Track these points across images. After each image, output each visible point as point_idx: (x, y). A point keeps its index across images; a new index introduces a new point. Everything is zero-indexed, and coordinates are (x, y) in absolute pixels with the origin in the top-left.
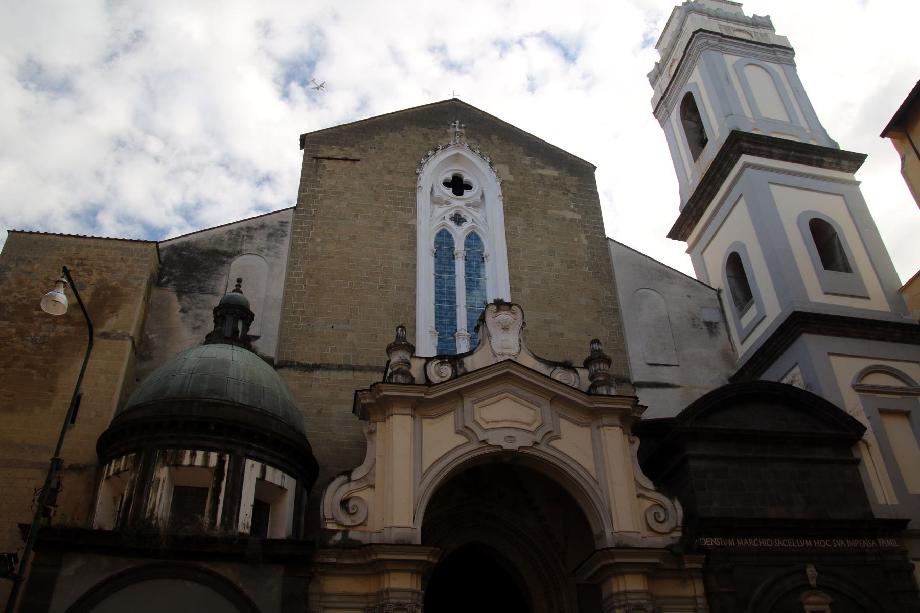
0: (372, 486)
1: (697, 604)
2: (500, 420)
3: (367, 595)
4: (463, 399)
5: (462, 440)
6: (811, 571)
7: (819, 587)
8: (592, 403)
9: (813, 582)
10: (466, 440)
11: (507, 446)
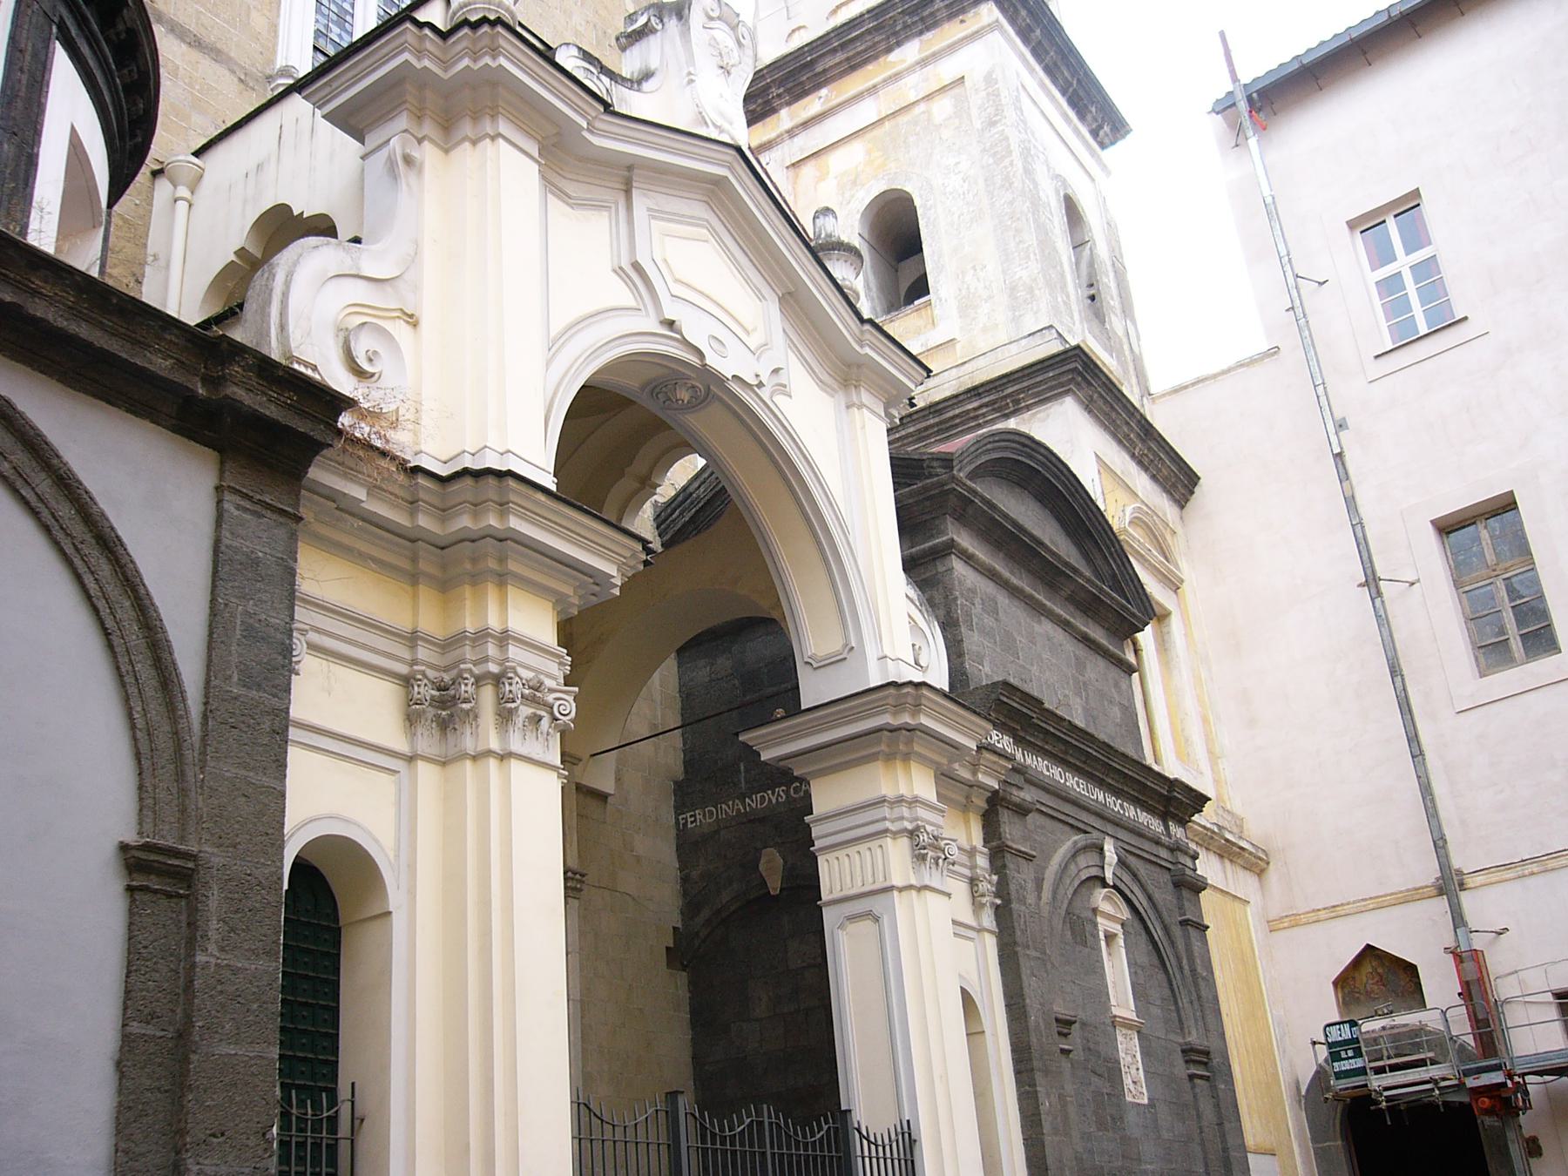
0: (411, 316)
1: (973, 867)
2: (699, 289)
3: (413, 639)
4: (628, 192)
5: (624, 296)
6: (1109, 847)
7: (1115, 887)
8: (861, 343)
9: (1109, 875)
10: (633, 303)
11: (712, 360)
